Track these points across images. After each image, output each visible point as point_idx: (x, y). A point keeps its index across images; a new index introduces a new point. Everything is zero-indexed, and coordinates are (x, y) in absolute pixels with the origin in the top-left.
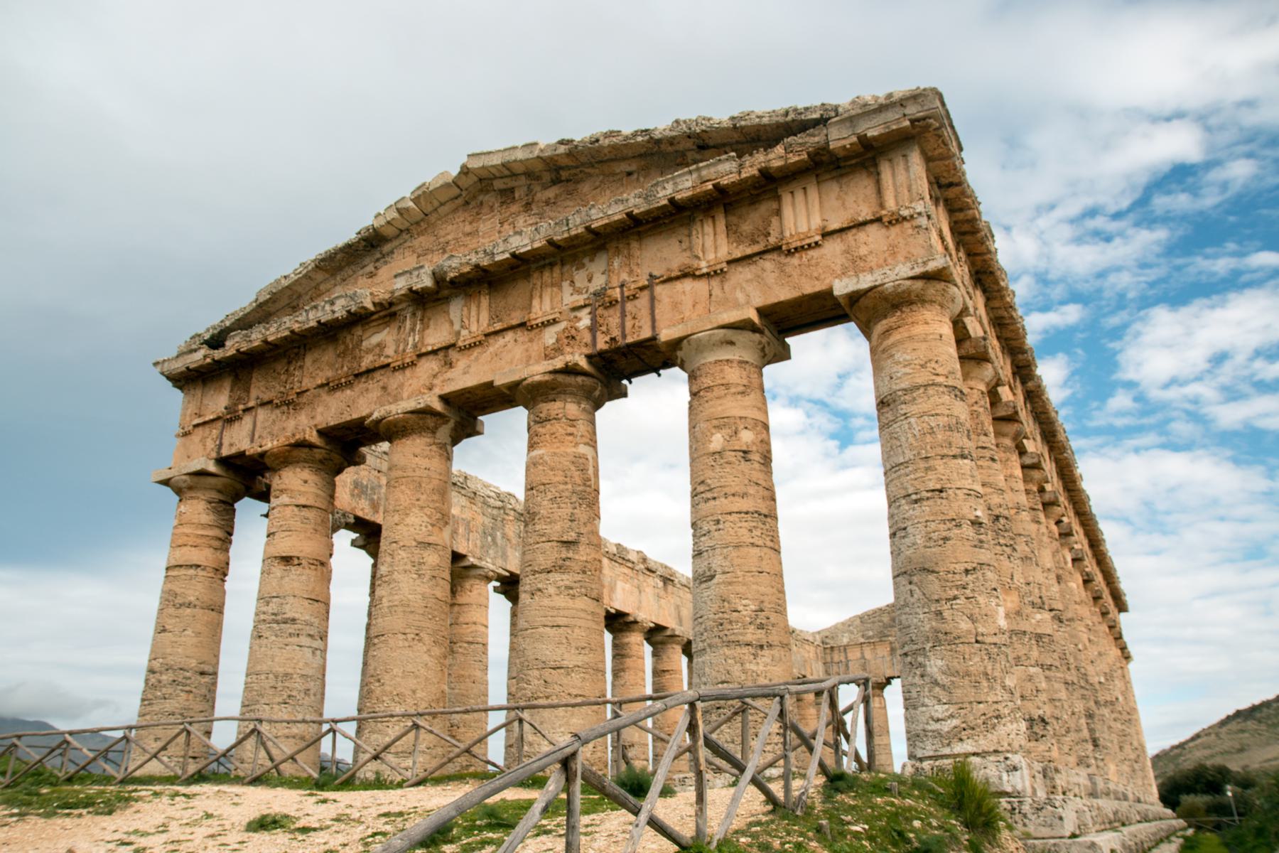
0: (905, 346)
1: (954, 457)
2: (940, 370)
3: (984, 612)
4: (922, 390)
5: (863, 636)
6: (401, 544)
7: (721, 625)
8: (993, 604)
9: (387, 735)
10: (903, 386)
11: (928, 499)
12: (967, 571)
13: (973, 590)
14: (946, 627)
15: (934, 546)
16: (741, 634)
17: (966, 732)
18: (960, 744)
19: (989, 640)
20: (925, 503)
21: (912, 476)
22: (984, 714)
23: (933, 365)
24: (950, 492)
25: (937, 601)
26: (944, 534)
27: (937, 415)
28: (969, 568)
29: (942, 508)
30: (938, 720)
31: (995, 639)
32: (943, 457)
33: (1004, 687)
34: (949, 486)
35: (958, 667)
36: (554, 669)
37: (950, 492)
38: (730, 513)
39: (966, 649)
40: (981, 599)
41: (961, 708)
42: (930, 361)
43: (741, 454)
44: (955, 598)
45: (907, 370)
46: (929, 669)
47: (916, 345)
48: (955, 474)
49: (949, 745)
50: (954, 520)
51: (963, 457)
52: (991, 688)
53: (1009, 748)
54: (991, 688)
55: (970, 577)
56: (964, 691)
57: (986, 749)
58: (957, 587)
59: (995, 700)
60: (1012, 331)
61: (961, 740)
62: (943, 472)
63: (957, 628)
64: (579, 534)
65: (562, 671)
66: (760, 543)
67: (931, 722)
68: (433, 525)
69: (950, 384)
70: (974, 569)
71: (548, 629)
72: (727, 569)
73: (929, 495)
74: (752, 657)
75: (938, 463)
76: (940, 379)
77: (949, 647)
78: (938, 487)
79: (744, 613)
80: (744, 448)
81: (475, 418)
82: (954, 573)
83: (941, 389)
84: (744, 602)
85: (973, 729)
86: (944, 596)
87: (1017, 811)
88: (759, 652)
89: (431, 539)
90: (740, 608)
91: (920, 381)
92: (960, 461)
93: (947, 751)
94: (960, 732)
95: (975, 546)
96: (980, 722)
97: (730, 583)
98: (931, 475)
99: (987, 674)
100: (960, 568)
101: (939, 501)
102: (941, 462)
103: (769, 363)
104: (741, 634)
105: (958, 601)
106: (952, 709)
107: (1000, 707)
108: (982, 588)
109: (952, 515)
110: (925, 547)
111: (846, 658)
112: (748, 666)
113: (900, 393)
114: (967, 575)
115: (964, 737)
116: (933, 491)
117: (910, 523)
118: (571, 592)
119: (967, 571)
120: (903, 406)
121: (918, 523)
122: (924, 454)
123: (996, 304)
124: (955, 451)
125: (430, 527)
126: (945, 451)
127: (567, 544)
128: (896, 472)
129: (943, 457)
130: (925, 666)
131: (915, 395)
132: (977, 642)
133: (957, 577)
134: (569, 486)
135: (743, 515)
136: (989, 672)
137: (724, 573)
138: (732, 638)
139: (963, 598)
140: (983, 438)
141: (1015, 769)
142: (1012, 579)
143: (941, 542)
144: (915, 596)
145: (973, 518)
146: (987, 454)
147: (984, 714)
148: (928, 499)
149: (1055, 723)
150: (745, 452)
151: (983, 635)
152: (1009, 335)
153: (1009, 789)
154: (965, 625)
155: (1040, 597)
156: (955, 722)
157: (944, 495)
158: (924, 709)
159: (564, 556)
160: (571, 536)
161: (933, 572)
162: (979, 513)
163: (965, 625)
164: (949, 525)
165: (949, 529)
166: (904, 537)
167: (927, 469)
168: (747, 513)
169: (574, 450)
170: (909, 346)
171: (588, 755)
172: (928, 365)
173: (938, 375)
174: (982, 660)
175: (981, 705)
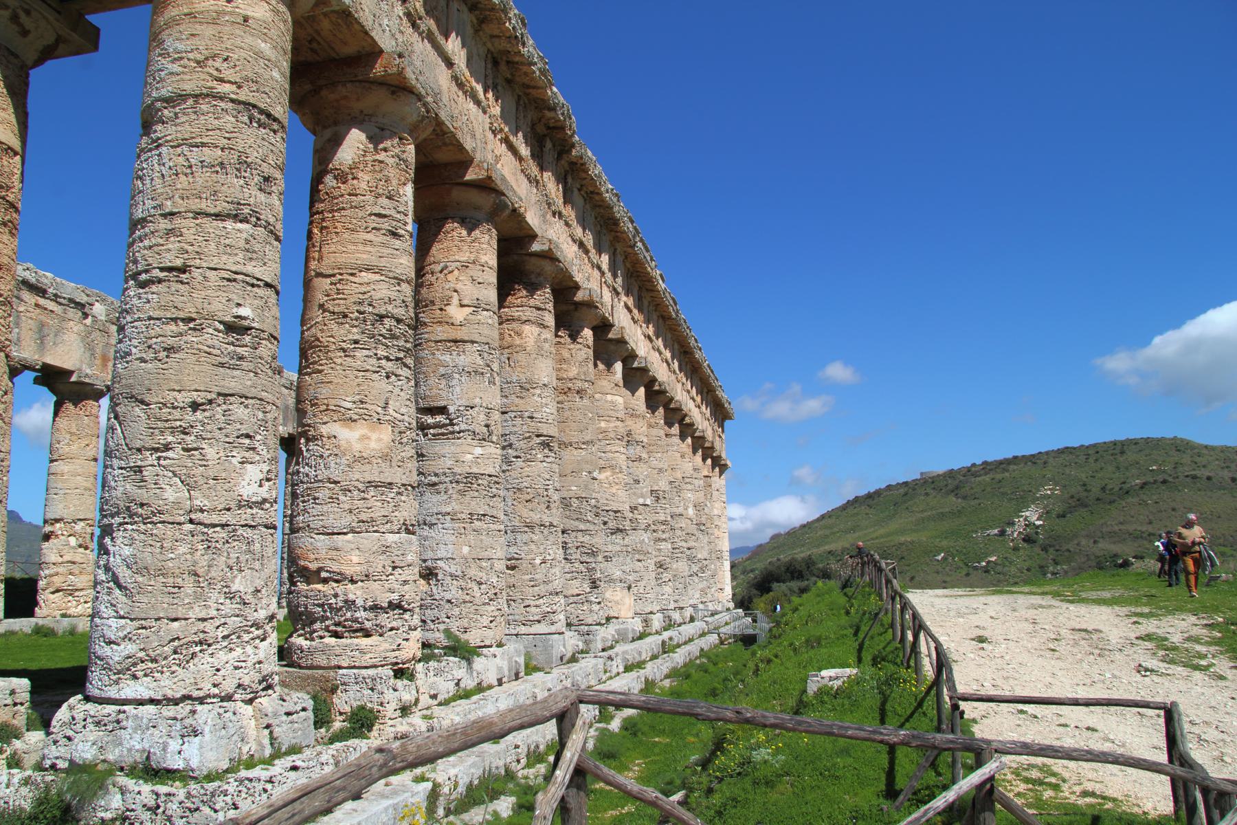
0: (182, 28)
1: (218, 216)
2: (228, 74)
3: (211, 473)
4: (190, 102)
10: (164, 92)
11: (160, 281)
12: (195, 406)
14: (142, 495)
17: (143, 666)
18: (131, 683)
19: (215, 519)
20: (154, 288)
21: (147, 243)
22: (178, 638)
23: (218, 64)
24: (196, 273)
25: (139, 450)
26: (171, 341)
27: (203, 145)
28: (200, 400)
29: (178, 300)
30: (110, 643)
31: (226, 518)
32: (198, 214)
33: (231, 596)
35: (149, 559)
39: (169, 531)
40: (210, 452)
42: (214, 57)
45: (176, 68)
46: (112, 559)
47: (198, 29)
48: (213, 245)
49: (117, 682)
50: (192, 320)
51: (236, 218)
52: (199, 597)
53: (216, 691)
54: (199, 597)
56: (154, 601)
57: (170, 694)
58: (173, 430)
59: (203, 615)
60: (526, 74)
61: (135, 677)
63: (158, 497)
69: (242, 98)
70: (210, 402)
73: (162, 275)
75: (187, 225)
76: (226, 88)
77: (143, 527)
82: (174, 408)
83: (222, 105)
85: (156, 661)
86: (150, 443)
87: (160, 810)
91: (189, 87)
92: (229, 224)
93: (112, 693)
94: (135, 664)
95: (222, 365)
96: (168, 649)
98: (173, 243)
99: (196, 575)
100: (184, 398)
101: (175, 286)
102: (191, 223)
103: (47, 54)
105: (170, 454)
106: (130, 626)
107: (208, 626)
108: (217, 434)
109: (190, 310)
110: (143, 360)
113: (158, 105)
114: (195, 411)
115: (140, 674)
116: (170, 269)
117: (129, 319)
119: (195, 406)
120: (159, 127)
121: (139, 319)
122: (169, 206)
123: (491, 29)
124: (222, 207)
126: (203, 205)
129: (198, 214)
131: (177, 110)
132: (191, 521)
133: (177, 414)
136: (200, 571)
140: (384, 201)
141: (195, 733)
142: (384, 408)
143: (163, 354)
145: (228, 319)
146: (386, 225)
147: (178, 638)
148: (160, 281)
149: (476, 588)
152: (526, 80)
153: (177, 763)
154: (172, 493)
155: (487, 426)
156: (129, 648)
161: (142, 402)
162: (244, 311)
163: (172, 493)
165: (181, 334)
167: (170, 232)
170: (186, 28)
172: (210, 62)
173: (222, 80)
174: (193, 551)
175: (176, 624)
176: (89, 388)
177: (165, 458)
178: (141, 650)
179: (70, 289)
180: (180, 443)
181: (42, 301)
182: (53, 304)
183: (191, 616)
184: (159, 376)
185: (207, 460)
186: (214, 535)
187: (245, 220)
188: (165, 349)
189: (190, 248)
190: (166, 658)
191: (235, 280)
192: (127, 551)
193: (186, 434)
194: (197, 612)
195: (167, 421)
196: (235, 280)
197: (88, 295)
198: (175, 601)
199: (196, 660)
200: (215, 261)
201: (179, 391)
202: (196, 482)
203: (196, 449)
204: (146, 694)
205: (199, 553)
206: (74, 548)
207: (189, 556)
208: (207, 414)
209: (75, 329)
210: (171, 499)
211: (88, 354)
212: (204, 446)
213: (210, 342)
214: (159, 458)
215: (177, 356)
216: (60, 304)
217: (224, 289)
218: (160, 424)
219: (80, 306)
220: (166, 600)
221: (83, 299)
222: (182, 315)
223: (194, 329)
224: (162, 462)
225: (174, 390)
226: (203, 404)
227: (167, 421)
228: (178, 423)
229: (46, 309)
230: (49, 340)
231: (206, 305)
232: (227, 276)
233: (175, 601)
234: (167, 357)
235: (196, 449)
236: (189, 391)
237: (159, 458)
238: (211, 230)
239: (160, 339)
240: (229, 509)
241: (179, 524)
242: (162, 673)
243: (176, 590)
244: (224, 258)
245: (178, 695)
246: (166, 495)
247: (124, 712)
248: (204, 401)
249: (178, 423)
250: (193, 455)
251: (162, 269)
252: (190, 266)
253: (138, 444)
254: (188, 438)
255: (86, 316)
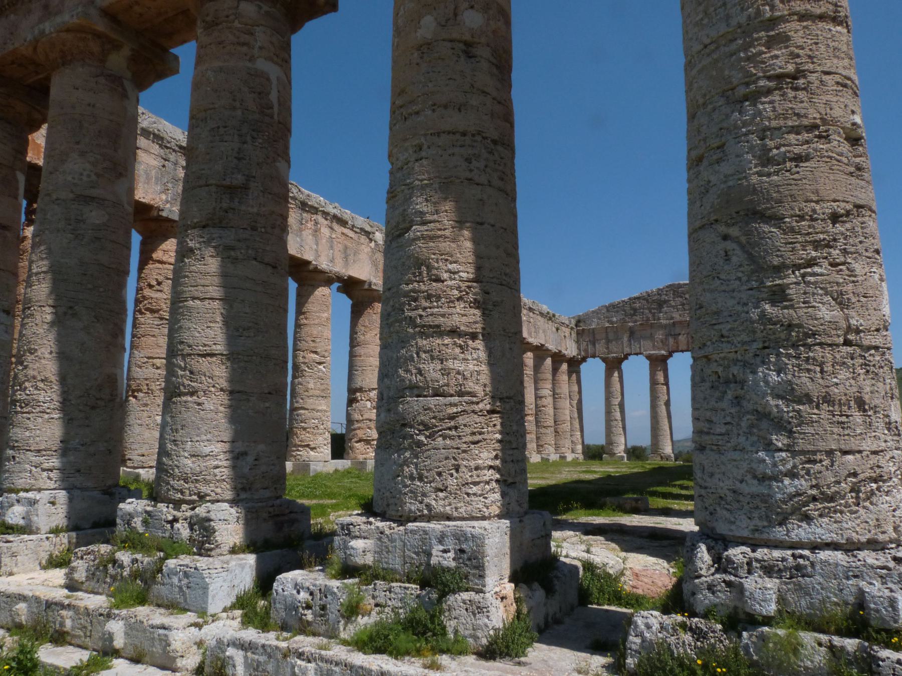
1: (822, 17)
5: (608, 322)
6: (54, 197)
7: (415, 300)
8: (877, 276)
9: (27, 429)
12: (835, 218)
13: (845, 252)
15: (777, 173)
16: (443, 316)
22: (855, 475)
29: (799, 107)
34: (811, 66)
36: (204, 356)
37: (812, 77)
38: (439, 134)
40: (858, 267)
41: (809, 461)
43: (461, 46)
44: (811, 263)
48: (823, 48)
50: (815, 127)
51: (836, 20)
55: (839, 228)
58: (817, 245)
59: (874, 448)
61: (807, 518)
62: (800, 42)
64: (249, 178)
65: (214, 359)
66: (483, 179)
67: (748, 478)
68: (98, 175)
70: (848, 213)
71: (198, 302)
72: (429, 217)
74: (458, 350)
78: (791, 68)
79: (449, 283)
80: (467, 37)
81: (165, 50)
84: (450, 267)
88: (470, 342)
89: (95, 192)
90: (445, 276)
94: (806, 504)
97: (432, 238)
100: (821, 209)
102: (795, 25)
104: (443, 316)
105: (817, 269)
110: (760, 174)
111: (594, 338)
112: (450, 364)
114: (834, 223)
118: (232, 253)
119: (835, 218)
125: (94, 177)
127: (232, 191)
128: (708, 55)
129: (803, 17)
130: (742, 383)
132: (847, 343)
134: (239, 112)
135: (458, 136)
136: (866, 398)
137: (424, 223)
138: (430, 320)
139: (825, 264)
144: (734, 259)
147: (855, 475)
150: (468, 44)
151: (858, 331)
154: (827, 312)
157: (801, 81)
158: (737, 455)
159: (225, 205)
160: (239, 179)
162: (858, 119)
163: (827, 312)
164: (806, 136)
165: (807, 142)
166: (718, 162)
168: (464, 134)
169: (249, 65)
171: (246, 470)
176: (375, 293)
177: (814, 274)
178: (812, 487)
179: (360, 221)
180: (826, 258)
181: (346, 231)
182: (351, 232)
183: (865, 448)
184: (790, 187)
185: (855, 276)
186: (871, 358)
187: (840, 24)
188: (791, 160)
189: (801, 52)
190: (843, 497)
191: (845, 86)
192: (774, 377)
193: (831, 247)
194: (868, 445)
195: (809, 234)
196: (845, 86)
197: (371, 226)
198: (846, 432)
199: (874, 499)
200: (828, 65)
201: (817, 202)
202: (848, 299)
203: (843, 264)
204: (828, 537)
205: (862, 377)
206: (370, 409)
207: (853, 382)
208: (848, 226)
209: (366, 250)
210: (828, 318)
211: (374, 269)
212: (849, 260)
213: (839, 150)
214: (803, 276)
215: (807, 164)
216: (356, 232)
217: (840, 94)
218: (800, 238)
219: (367, 234)
220: (835, 430)
221: (368, 228)
222: (806, 122)
223: (820, 137)
224: (809, 278)
225: (812, 201)
226: (842, 216)
227: (809, 234)
228: (822, 236)
229: (348, 236)
230: (351, 257)
231: (828, 111)
232: (840, 80)
233: (846, 432)
234: (796, 166)
235: (843, 264)
236: (828, 201)
237: (803, 276)
238: (819, 33)
239: (783, 149)
240: (878, 330)
241: (838, 345)
242: (841, 512)
243: (844, 419)
244: (835, 61)
245: (863, 539)
246: (820, 314)
247: (801, 556)
248: (842, 211)
249: (822, 236)
250: (841, 270)
251: (769, 78)
252: (804, 71)
253: (776, 261)
254: (835, 252)
255: (371, 240)
